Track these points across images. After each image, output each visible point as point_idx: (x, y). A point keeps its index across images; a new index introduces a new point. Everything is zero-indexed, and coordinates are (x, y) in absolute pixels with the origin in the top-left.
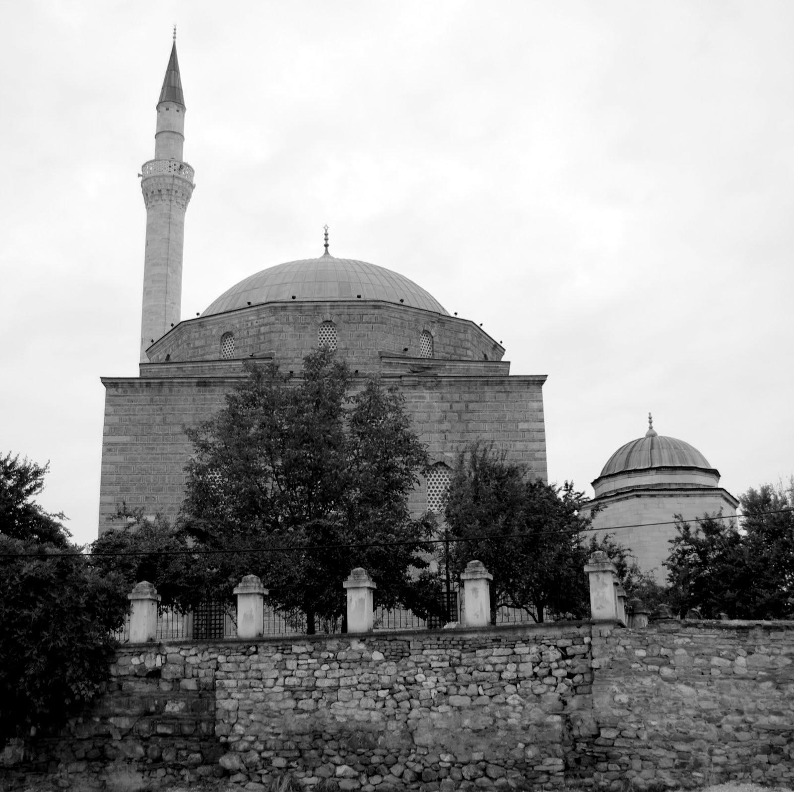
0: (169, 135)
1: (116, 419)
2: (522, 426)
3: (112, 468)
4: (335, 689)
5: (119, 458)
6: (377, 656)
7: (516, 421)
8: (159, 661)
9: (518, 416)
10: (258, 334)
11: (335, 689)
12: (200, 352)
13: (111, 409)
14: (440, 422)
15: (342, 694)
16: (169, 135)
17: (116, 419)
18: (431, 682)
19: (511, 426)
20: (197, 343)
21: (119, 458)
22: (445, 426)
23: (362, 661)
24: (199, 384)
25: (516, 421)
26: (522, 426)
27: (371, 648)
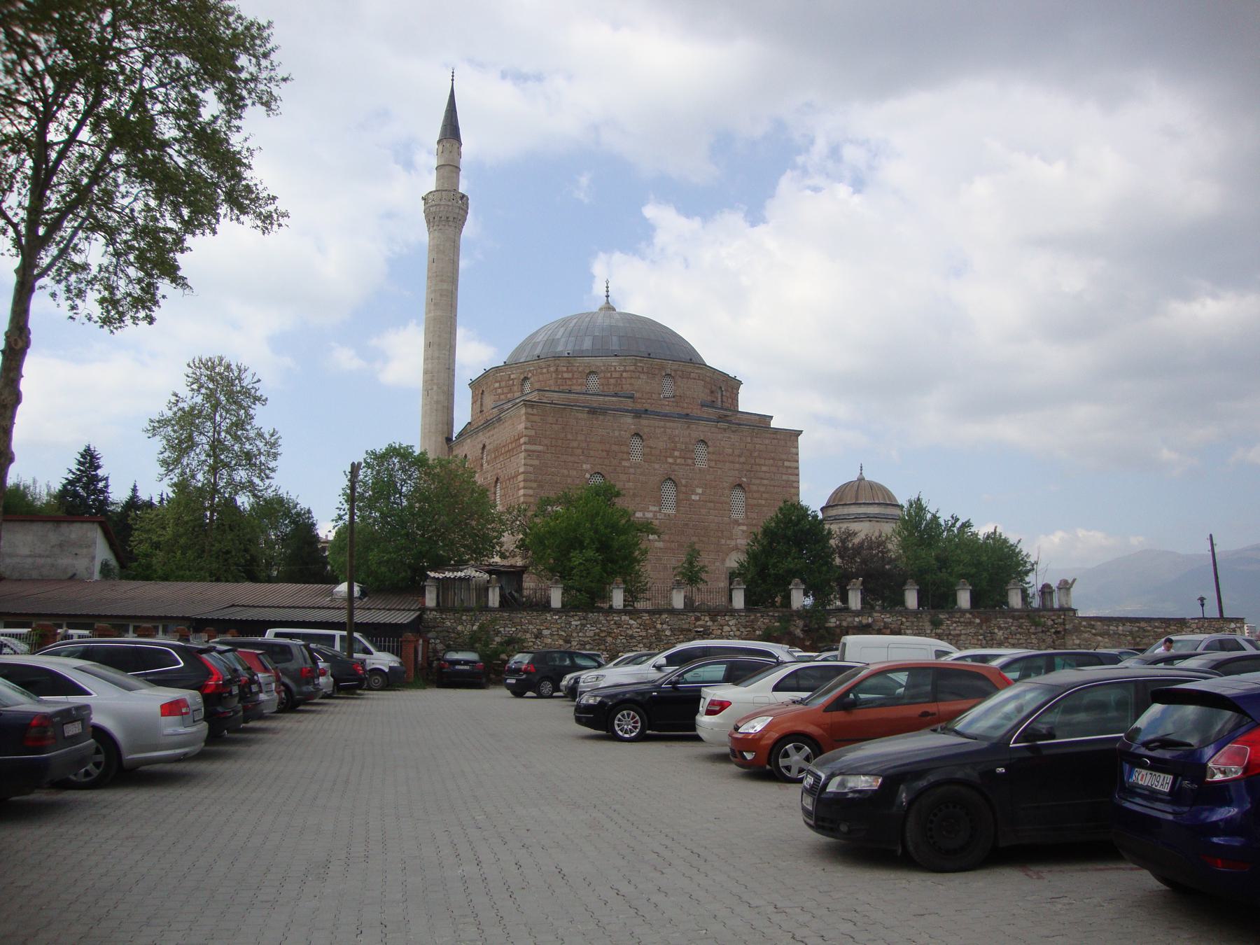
0: (450, 167)
1: (533, 433)
2: (787, 464)
3: (531, 469)
4: (959, 635)
5: (536, 462)
6: (978, 621)
7: (784, 460)
8: (870, 620)
9: (784, 457)
10: (621, 377)
11: (959, 635)
12: (569, 382)
13: (529, 425)
14: (739, 456)
15: (963, 637)
16: (450, 167)
17: (533, 433)
18: (1001, 633)
19: (780, 463)
20: (566, 375)
21: (536, 462)
22: (742, 460)
23: (970, 623)
24: (589, 412)
25: (784, 460)
26: (787, 464)
27: (974, 617)
